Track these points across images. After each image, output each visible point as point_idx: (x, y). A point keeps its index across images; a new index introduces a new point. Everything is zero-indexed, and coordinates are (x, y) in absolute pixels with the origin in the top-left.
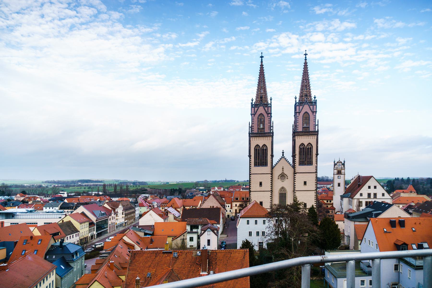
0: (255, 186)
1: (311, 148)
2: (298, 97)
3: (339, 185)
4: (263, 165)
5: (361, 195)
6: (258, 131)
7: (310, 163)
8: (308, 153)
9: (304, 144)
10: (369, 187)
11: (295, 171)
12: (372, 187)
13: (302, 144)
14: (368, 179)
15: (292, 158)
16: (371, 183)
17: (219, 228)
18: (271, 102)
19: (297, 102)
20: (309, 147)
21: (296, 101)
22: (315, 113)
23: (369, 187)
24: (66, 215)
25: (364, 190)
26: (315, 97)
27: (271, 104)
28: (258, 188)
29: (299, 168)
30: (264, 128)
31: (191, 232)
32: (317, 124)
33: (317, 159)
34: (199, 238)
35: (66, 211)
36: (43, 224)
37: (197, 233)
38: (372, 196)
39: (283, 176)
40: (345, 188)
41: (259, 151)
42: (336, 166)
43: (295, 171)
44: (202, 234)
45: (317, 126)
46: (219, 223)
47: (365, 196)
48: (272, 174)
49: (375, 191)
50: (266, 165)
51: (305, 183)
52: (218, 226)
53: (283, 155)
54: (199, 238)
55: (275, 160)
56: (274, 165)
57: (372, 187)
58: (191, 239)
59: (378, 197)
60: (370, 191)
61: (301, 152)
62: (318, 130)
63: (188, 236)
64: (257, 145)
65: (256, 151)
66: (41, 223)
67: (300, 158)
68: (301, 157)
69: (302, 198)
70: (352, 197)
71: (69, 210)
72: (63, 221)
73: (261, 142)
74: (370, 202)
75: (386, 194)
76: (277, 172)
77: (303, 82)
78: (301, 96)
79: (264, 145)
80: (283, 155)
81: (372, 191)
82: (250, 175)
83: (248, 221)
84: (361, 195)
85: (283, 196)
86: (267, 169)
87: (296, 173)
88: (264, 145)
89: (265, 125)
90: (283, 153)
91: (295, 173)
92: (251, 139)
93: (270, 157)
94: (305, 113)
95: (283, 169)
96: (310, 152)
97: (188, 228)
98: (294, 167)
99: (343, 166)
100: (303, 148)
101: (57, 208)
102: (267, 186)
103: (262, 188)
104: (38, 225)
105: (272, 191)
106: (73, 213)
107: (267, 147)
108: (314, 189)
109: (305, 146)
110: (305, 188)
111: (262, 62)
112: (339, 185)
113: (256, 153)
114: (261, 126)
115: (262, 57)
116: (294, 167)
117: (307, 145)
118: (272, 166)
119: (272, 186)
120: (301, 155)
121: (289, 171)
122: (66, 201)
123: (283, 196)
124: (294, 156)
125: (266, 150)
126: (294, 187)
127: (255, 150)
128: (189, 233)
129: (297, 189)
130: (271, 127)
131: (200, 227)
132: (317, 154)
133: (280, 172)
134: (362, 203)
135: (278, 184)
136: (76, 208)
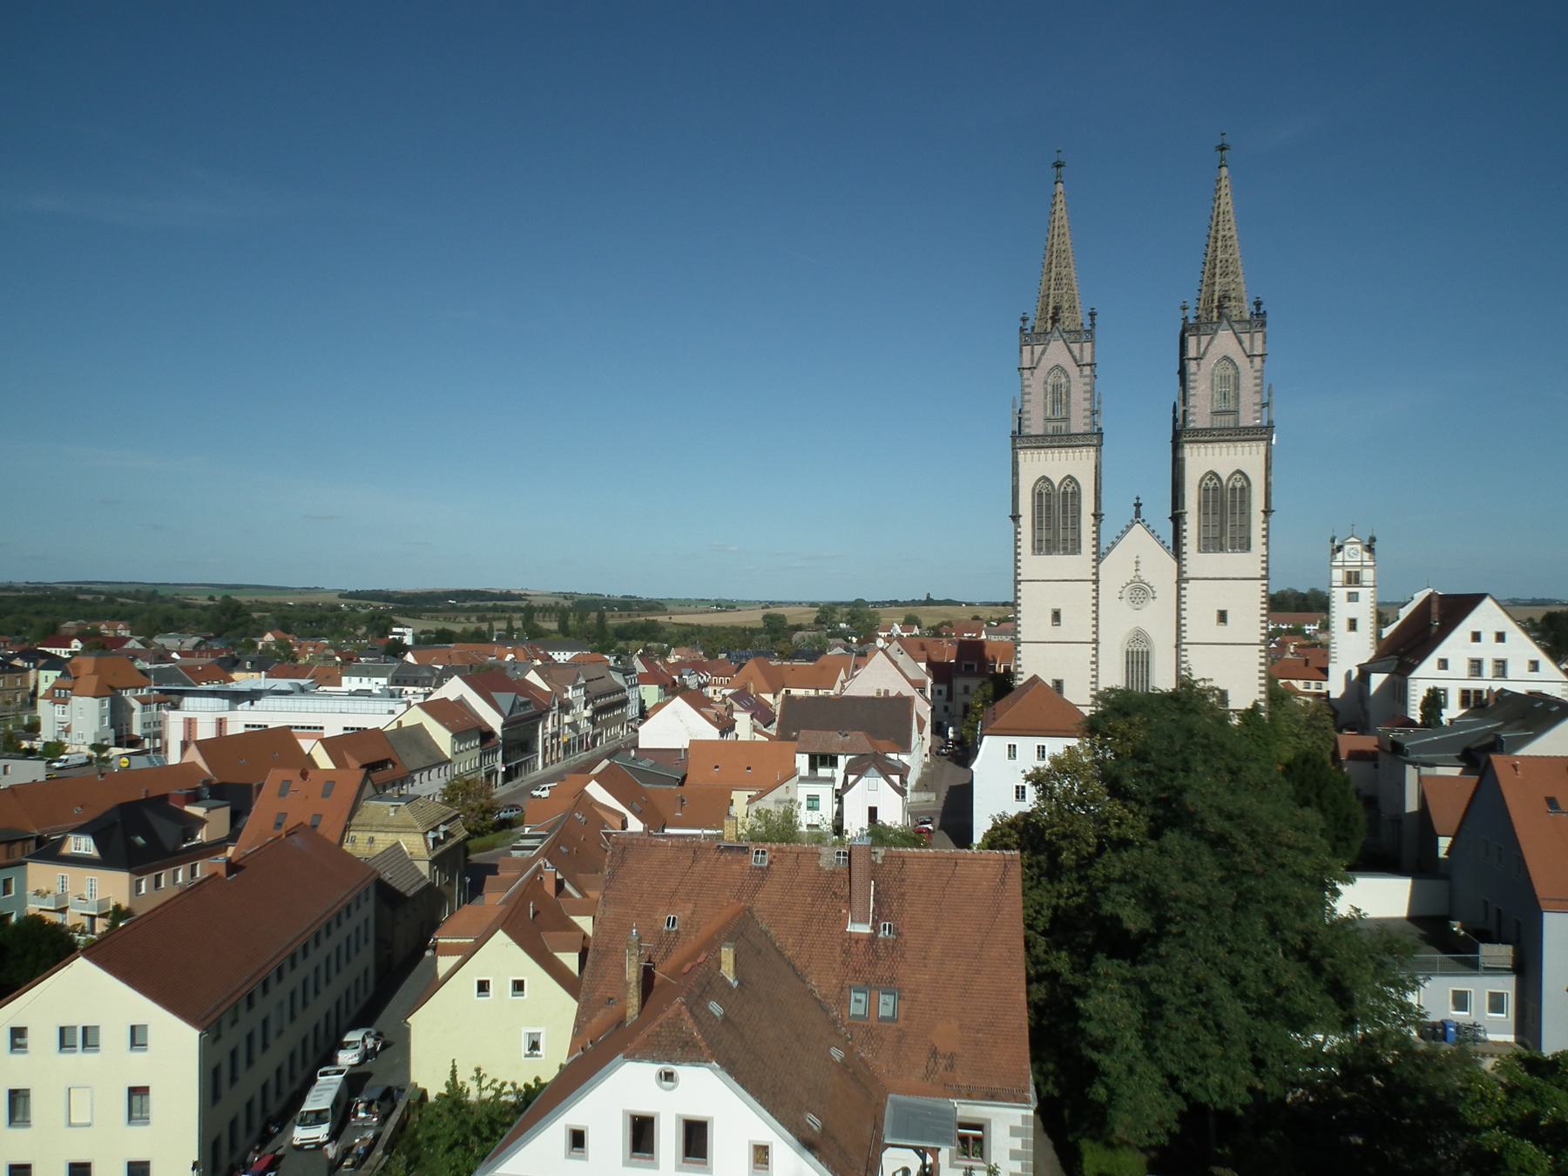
0: (1032, 622)
1: (1245, 492)
3: (1353, 625)
5: (1443, 664)
8: (1233, 506)
9: (1216, 475)
10: (1476, 637)
11: (1180, 572)
12: (1488, 637)
13: (1213, 475)
15: (1170, 524)
16: (1488, 616)
17: (907, 768)
20: (1238, 485)
23: (1476, 637)
24: (409, 703)
25: (1456, 646)
28: (1046, 630)
29: (1196, 561)
30: (1066, 419)
31: (813, 779)
34: (839, 796)
35: (410, 689)
36: (341, 732)
37: (832, 780)
38: (1488, 669)
40: (1379, 635)
42: (1339, 556)
44: (846, 786)
46: (905, 747)
47: (1459, 667)
48: (1096, 582)
49: (1500, 651)
50: (1075, 548)
51: (1223, 617)
52: (904, 758)
53: (1138, 514)
54: (839, 796)
57: (1488, 637)
58: (813, 801)
59: (1511, 673)
60: (1477, 651)
61: (1206, 502)
63: (803, 792)
64: (1045, 479)
65: (1040, 501)
66: (333, 729)
68: (1206, 520)
69: (1208, 668)
71: (420, 690)
72: (400, 723)
74: (1479, 692)
75: (1546, 663)
80: (1138, 514)
81: (1488, 651)
83: (1012, 748)
84: (1443, 664)
85: (1138, 661)
86: (1080, 564)
87: (1187, 580)
89: (1073, 409)
91: (1181, 579)
92: (1021, 455)
95: (1138, 505)
96: (1242, 502)
97: (802, 762)
99: (1366, 555)
100: (1215, 489)
101: (383, 681)
102: (1077, 623)
103: (1062, 632)
104: (327, 734)
105: (1096, 641)
106: (431, 698)
107: (1077, 484)
108: (1259, 638)
109: (1219, 479)
110: (1222, 633)
112: (1353, 625)
113: (1040, 506)
119: (1096, 626)
120: (1206, 514)
122: (410, 658)
123: (1138, 661)
125: (1076, 494)
127: (1038, 496)
128: (803, 780)
129: (1189, 636)
131: (842, 761)
134: (1445, 695)
136: (439, 684)
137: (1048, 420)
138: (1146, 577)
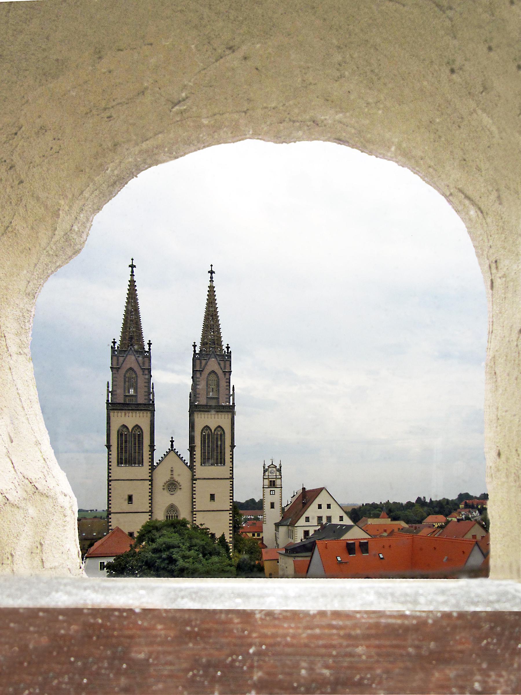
2: (198, 345)
4: (135, 463)
6: (125, 400)
7: (222, 462)
9: (209, 427)
11: (193, 475)
13: (207, 427)
14: (317, 492)
18: (150, 349)
19: (197, 352)
21: (195, 351)
22: (227, 374)
26: (228, 348)
27: (149, 352)
28: (126, 506)
29: (201, 471)
30: (136, 396)
32: (231, 393)
33: (232, 455)
39: (172, 486)
41: (126, 438)
43: (193, 475)
45: (231, 397)
48: (151, 481)
53: (172, 446)
55: (158, 456)
56: (155, 464)
62: (233, 403)
67: (203, 454)
70: (292, 525)
73: (131, 420)
76: (162, 477)
77: (206, 319)
78: (204, 344)
79: (137, 427)
80: (172, 446)
82: (109, 481)
86: (143, 471)
88: (137, 427)
89: (139, 390)
90: (172, 442)
91: (193, 479)
92: (112, 414)
93: (148, 448)
94: (210, 373)
98: (191, 467)
105: (151, 511)
107: (141, 429)
109: (211, 430)
110: (213, 506)
111: (132, 275)
113: (122, 440)
114: (132, 392)
115: (132, 266)
116: (191, 467)
117: (215, 430)
118: (152, 465)
121: (183, 476)
124: (192, 449)
125: (141, 436)
126: (193, 505)
127: (120, 434)
130: (149, 391)
132: (233, 446)
133: (167, 478)
135: (163, 500)
137: (126, 396)
138: (176, 478)
